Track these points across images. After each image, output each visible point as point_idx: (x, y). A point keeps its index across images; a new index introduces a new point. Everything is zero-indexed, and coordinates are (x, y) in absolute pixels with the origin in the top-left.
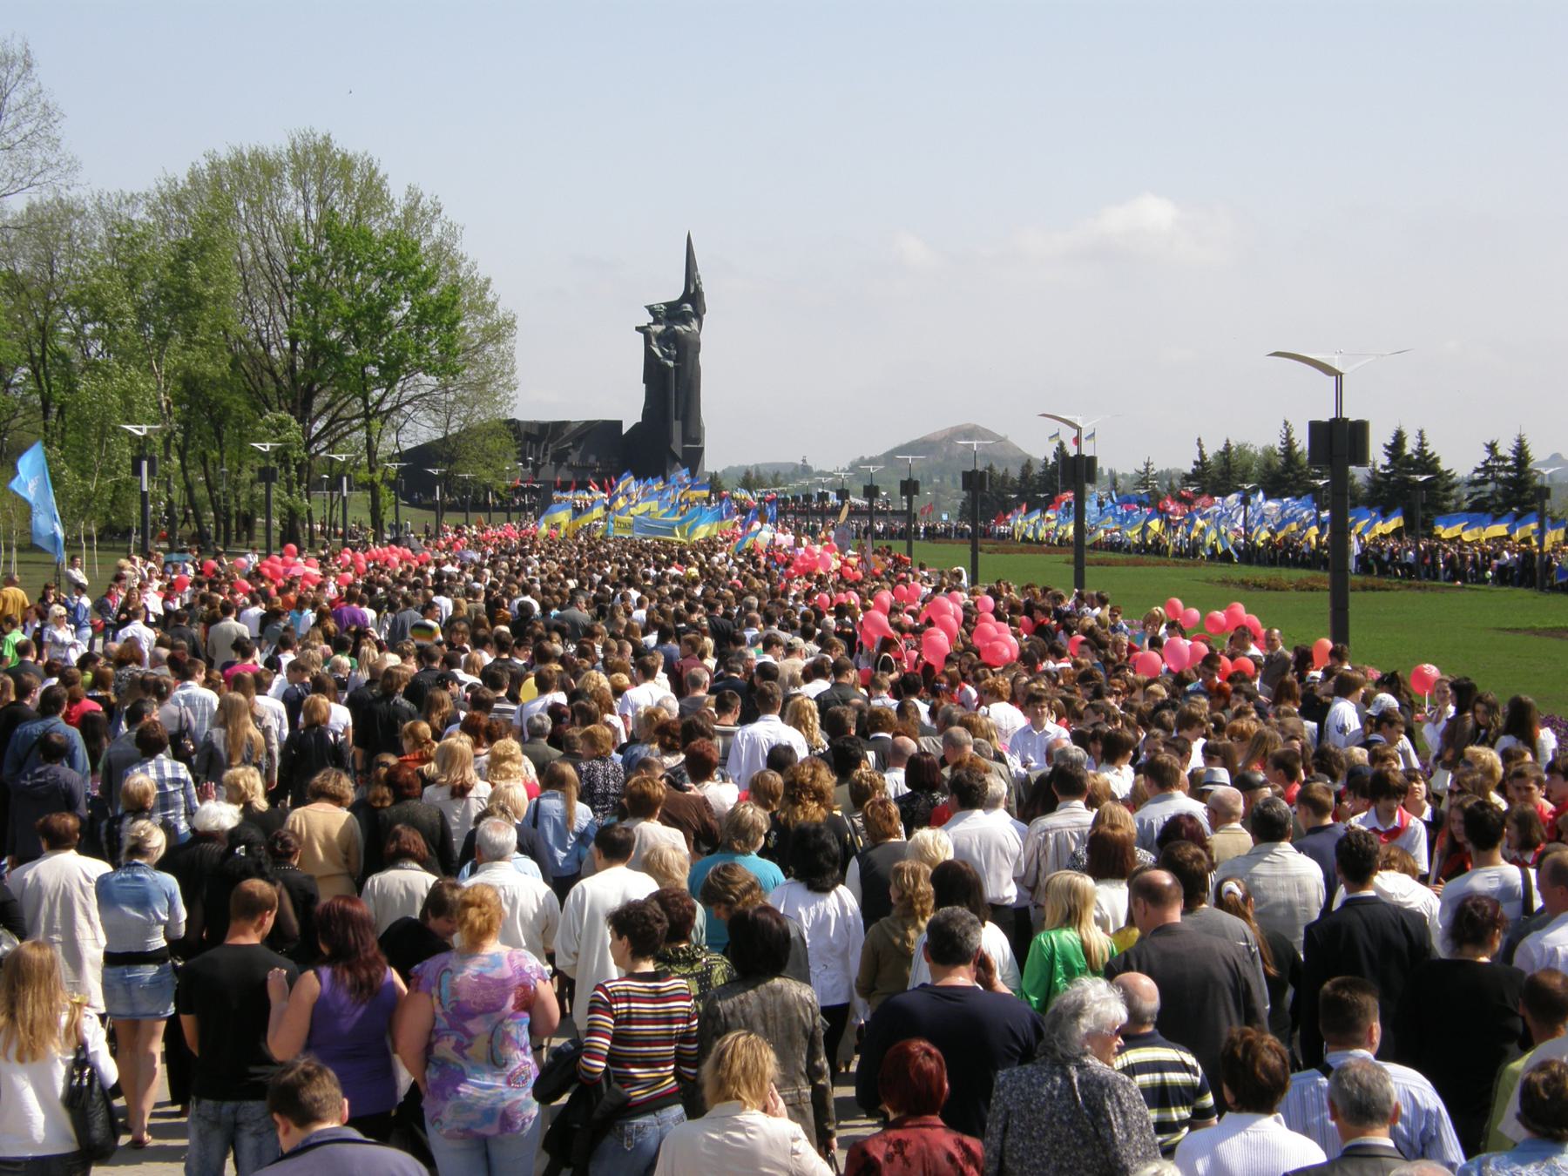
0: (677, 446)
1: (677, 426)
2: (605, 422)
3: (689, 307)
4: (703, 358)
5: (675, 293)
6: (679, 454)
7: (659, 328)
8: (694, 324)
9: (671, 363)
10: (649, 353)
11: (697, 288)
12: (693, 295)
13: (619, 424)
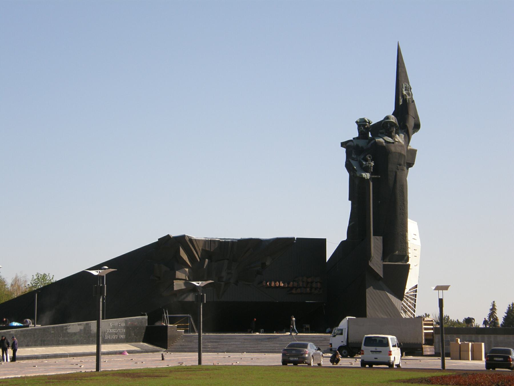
0: (377, 263)
1: (376, 244)
2: (301, 240)
6: (380, 273)
9: (367, 175)
13: (321, 243)
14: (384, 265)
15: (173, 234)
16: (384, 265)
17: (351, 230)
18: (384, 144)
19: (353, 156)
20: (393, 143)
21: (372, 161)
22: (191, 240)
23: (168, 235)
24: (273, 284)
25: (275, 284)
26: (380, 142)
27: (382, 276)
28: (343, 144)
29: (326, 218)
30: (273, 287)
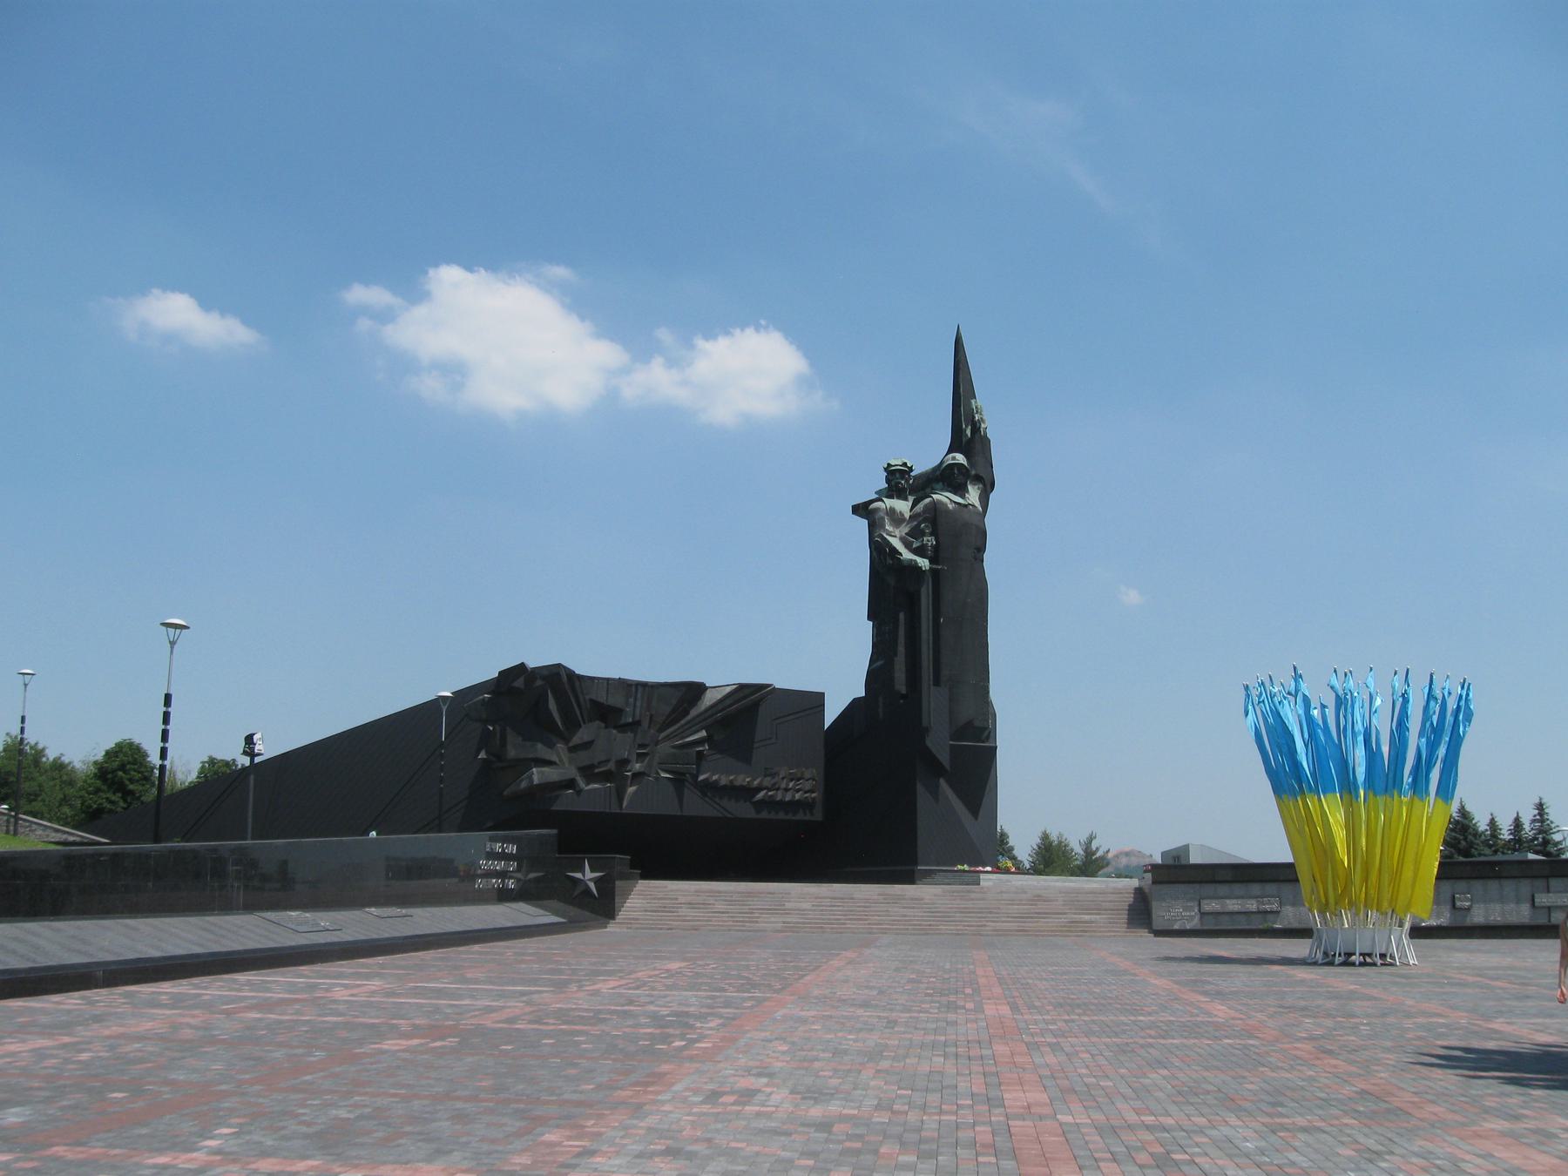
0: (939, 743)
1: (934, 703)
3: (960, 458)
4: (994, 563)
5: (928, 449)
6: (944, 758)
7: (903, 506)
8: (973, 495)
9: (924, 563)
10: (881, 553)
11: (976, 428)
12: (968, 436)
17: (876, 677)
18: (951, 506)
21: (931, 534)
22: (571, 675)
23: (523, 664)
26: (940, 502)
28: (861, 510)
29: (826, 655)
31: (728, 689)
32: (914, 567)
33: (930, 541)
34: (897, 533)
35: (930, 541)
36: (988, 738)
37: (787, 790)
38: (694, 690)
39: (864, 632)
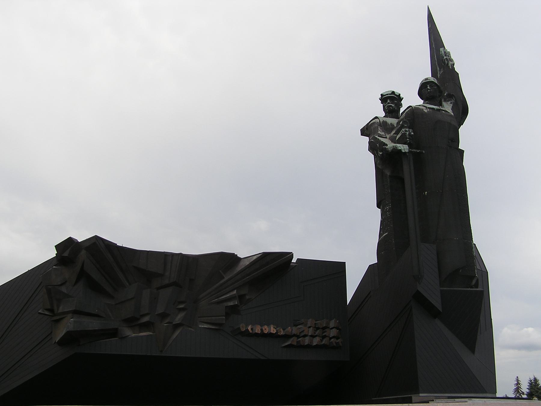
6: (436, 301)
9: (404, 148)
13: (339, 269)
14: (441, 291)
15: (81, 237)
16: (441, 291)
17: (383, 248)
18: (426, 111)
19: (379, 132)
20: (439, 110)
24: (258, 330)
25: (262, 330)
27: (440, 309)
29: (345, 234)
30: (256, 335)
31: (255, 258)
32: (397, 152)
33: (407, 131)
34: (388, 136)
35: (407, 131)
36: (476, 286)
37: (313, 336)
38: (227, 260)
39: (375, 216)
